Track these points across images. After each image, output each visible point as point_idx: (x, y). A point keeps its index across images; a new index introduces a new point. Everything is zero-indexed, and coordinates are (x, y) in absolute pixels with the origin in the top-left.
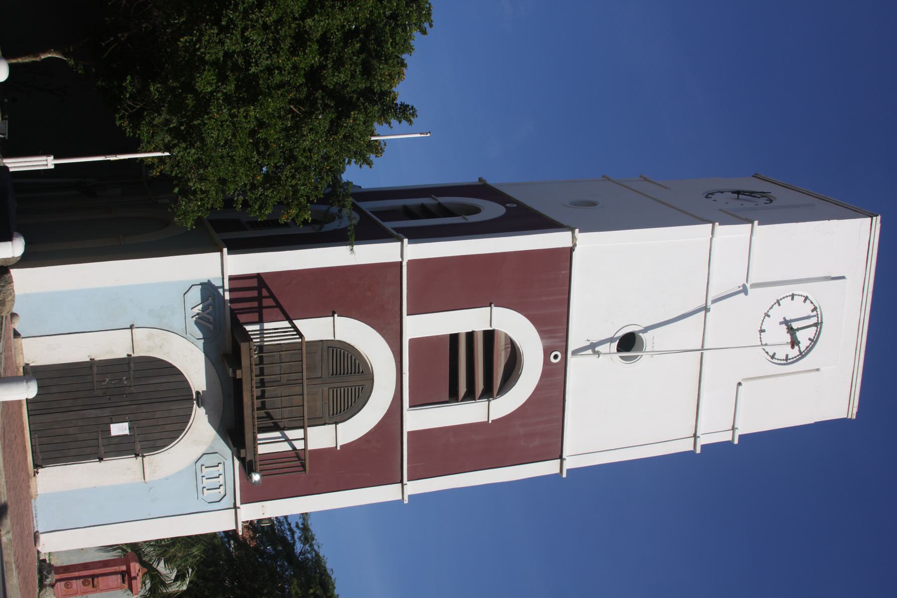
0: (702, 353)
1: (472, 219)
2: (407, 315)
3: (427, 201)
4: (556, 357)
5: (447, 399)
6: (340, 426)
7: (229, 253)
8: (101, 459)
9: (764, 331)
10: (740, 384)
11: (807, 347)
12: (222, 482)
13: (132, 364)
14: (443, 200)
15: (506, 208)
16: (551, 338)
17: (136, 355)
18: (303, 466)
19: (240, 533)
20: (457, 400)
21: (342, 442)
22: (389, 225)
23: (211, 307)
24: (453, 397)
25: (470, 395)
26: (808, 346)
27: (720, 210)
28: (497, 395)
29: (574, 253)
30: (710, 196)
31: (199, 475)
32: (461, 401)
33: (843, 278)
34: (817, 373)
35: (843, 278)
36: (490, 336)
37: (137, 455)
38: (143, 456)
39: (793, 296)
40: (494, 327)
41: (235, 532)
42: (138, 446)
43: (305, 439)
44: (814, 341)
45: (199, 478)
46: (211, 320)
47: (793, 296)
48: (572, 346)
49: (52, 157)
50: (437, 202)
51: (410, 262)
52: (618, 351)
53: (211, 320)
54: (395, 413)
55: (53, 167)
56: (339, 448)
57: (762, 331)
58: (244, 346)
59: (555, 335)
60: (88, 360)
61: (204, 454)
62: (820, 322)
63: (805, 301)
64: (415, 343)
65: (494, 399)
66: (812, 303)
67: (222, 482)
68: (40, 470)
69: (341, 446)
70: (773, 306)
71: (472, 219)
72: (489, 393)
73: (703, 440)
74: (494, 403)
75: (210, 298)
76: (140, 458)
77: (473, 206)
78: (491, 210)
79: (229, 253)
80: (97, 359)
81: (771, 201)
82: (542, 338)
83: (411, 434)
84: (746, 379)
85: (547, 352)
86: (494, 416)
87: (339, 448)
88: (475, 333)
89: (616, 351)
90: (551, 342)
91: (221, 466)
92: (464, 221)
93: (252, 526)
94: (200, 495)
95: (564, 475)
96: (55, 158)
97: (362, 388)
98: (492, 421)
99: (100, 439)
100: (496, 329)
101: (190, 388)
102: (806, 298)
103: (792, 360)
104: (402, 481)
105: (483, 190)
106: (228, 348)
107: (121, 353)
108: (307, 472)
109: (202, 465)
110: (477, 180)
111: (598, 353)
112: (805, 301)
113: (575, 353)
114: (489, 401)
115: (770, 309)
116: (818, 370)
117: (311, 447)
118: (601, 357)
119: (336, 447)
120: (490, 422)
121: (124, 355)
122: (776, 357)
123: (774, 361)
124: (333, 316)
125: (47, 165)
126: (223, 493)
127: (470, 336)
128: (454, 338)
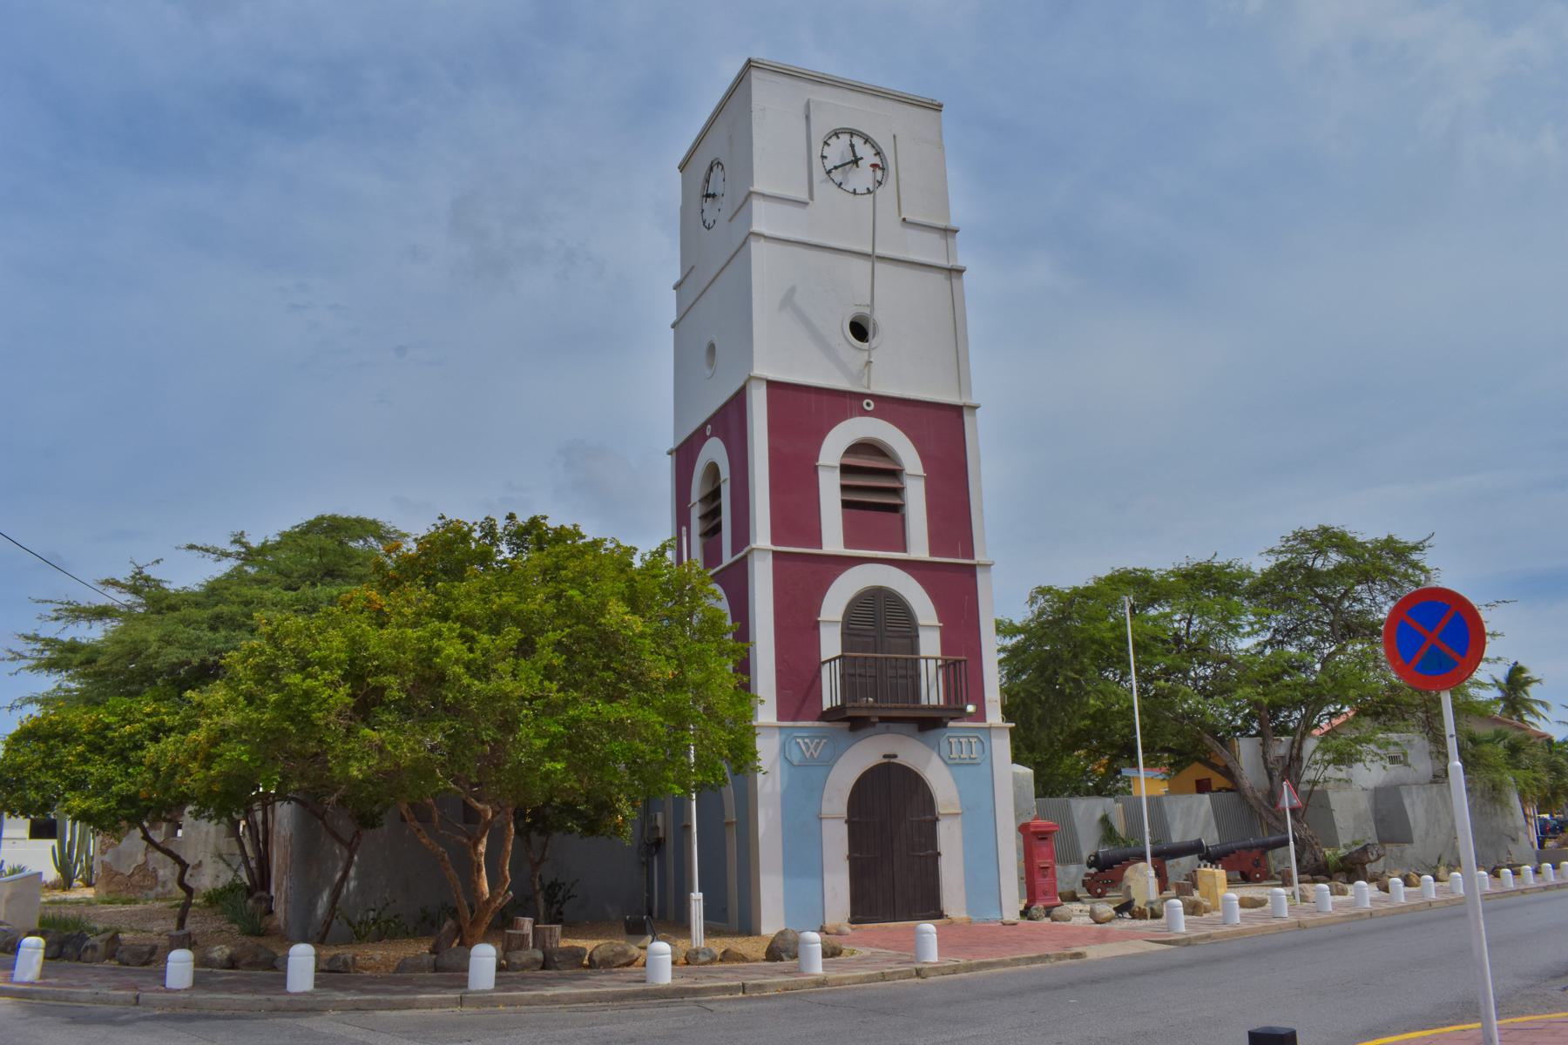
0: (879, 258)
1: (725, 473)
3: (696, 513)
4: (868, 404)
5: (897, 516)
6: (921, 621)
8: (939, 854)
9: (855, 190)
10: (904, 220)
12: (966, 740)
13: (855, 819)
14: (696, 493)
15: (711, 436)
17: (846, 816)
18: (960, 662)
19: (1013, 725)
20: (903, 506)
22: (727, 559)
23: (806, 740)
24: (897, 509)
25: (898, 492)
27: (730, 220)
29: (770, 378)
30: (707, 224)
31: (957, 761)
34: (897, 139)
36: (846, 470)
37: (937, 819)
38: (939, 813)
39: (823, 157)
40: (839, 466)
41: (1011, 730)
42: (929, 817)
43: (936, 659)
44: (867, 140)
45: (961, 762)
46: (817, 740)
47: (823, 157)
49: (693, 894)
50: (698, 503)
51: (775, 541)
52: (867, 341)
53: (817, 740)
54: (911, 567)
55: (701, 894)
56: (941, 625)
57: (854, 192)
58: (850, 713)
60: (848, 862)
61: (939, 755)
63: (829, 145)
64: (848, 543)
66: (830, 138)
67: (966, 740)
68: (945, 913)
69: (940, 622)
71: (725, 473)
72: (895, 473)
75: (798, 740)
76: (940, 818)
77: (705, 471)
78: (714, 451)
80: (847, 853)
81: (719, 163)
83: (932, 552)
84: (900, 215)
86: (919, 470)
87: (941, 625)
89: (867, 344)
91: (951, 740)
92: (728, 482)
93: (1008, 714)
94: (978, 761)
96: (692, 890)
98: (925, 472)
99: (921, 854)
101: (881, 764)
102: (826, 143)
104: (973, 567)
105: (685, 454)
106: (847, 725)
107: (843, 830)
108: (964, 657)
109: (949, 758)
110: (670, 456)
112: (829, 145)
115: (834, 181)
116: (894, 137)
117: (938, 654)
118: (872, 360)
121: (845, 828)
122: (880, 180)
124: (819, 622)
125: (699, 900)
126: (976, 740)
127: (844, 488)
128: (846, 504)
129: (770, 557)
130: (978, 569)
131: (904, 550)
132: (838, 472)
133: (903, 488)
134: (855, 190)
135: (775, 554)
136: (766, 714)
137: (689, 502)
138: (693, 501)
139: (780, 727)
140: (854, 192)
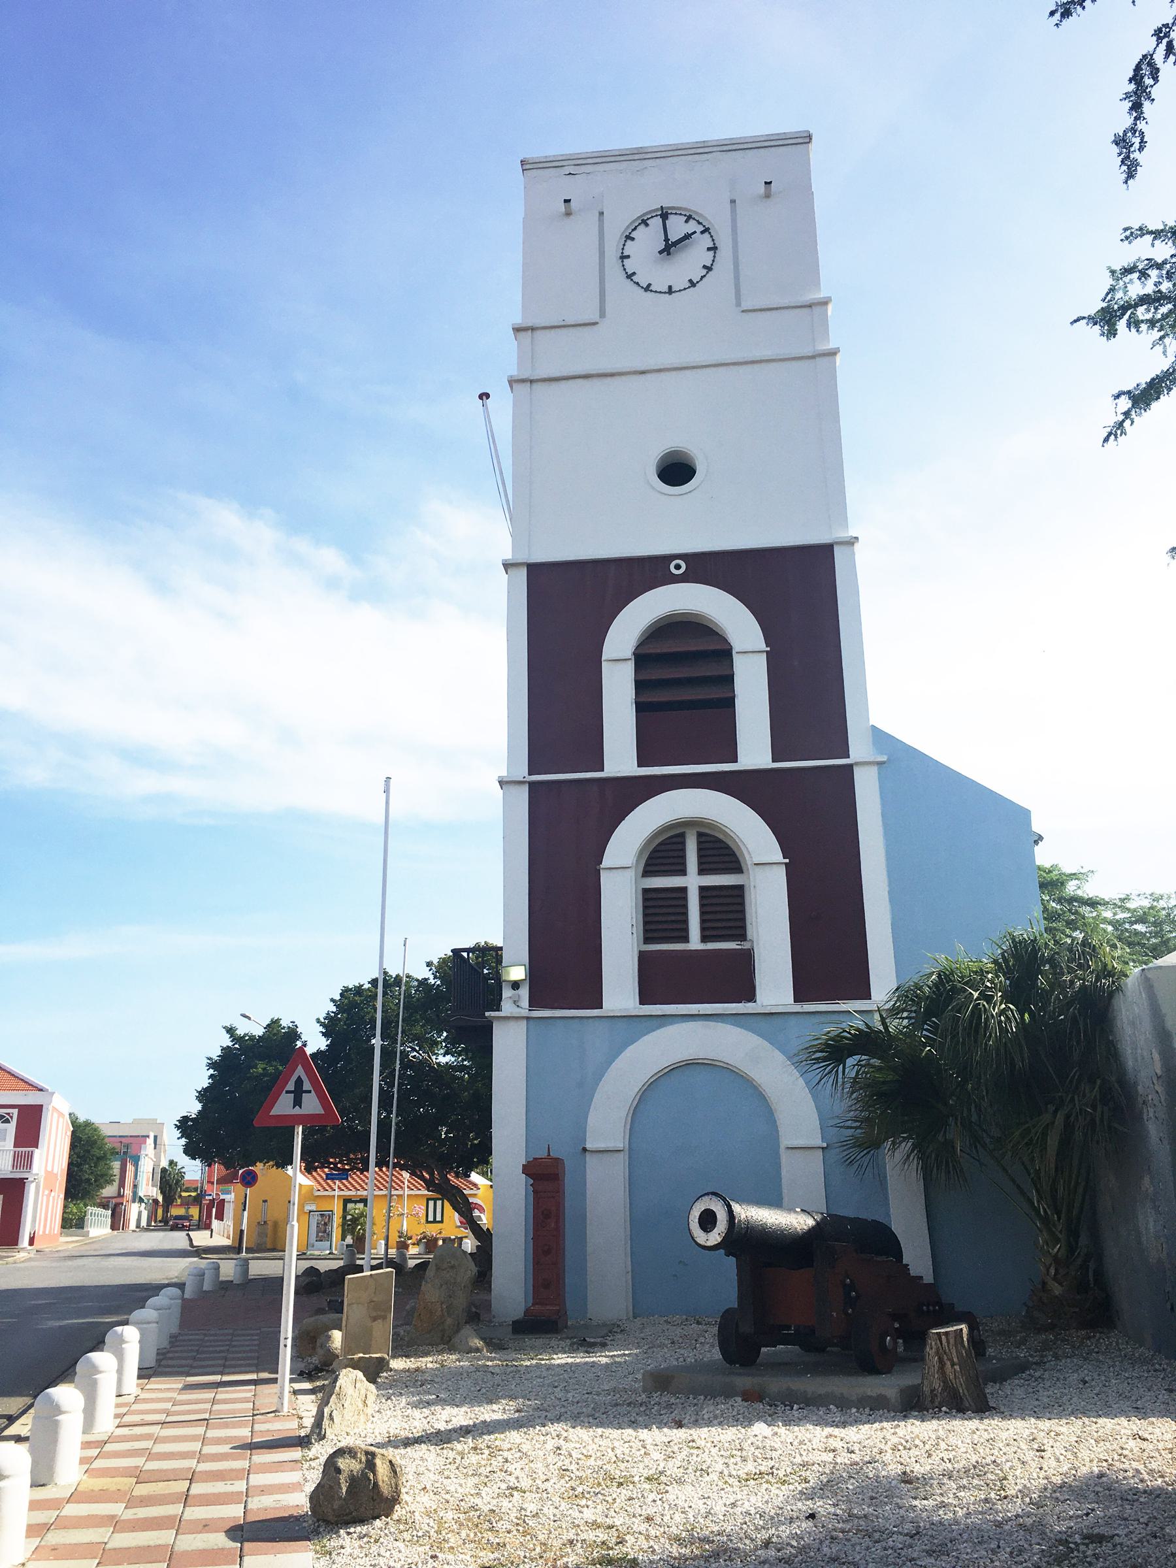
4: (678, 567)
7: (499, 1009)
21: (777, 856)
24: (729, 703)
25: (729, 680)
36: (642, 659)
56: (787, 861)
72: (724, 654)
74: (737, 644)
79: (499, 1009)
87: (787, 861)
104: (849, 768)
119: (786, 864)
120: (768, 649)
127: (640, 685)
128: (641, 708)
129: (526, 788)
130: (858, 773)
131: (735, 760)
132: (630, 668)
135: (533, 786)
136: (516, 1003)
139: (528, 1018)
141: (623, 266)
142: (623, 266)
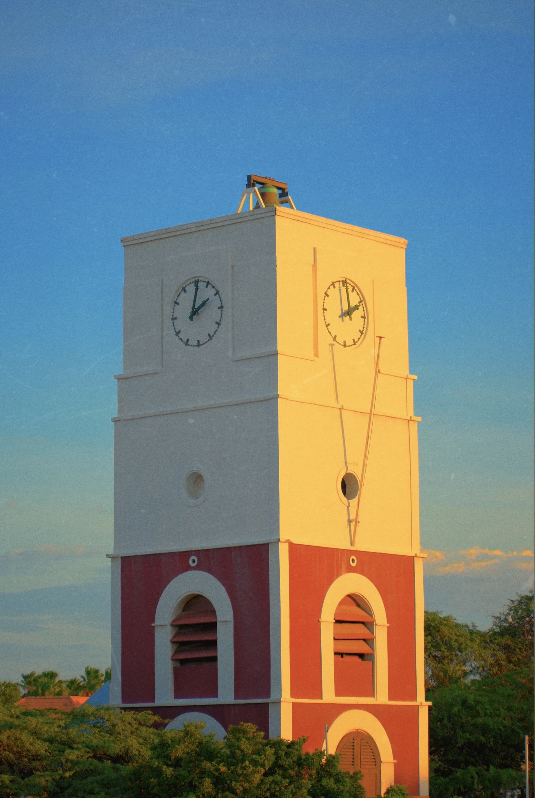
2: (322, 699)
4: (353, 560)
6: (382, 759)
9: (345, 342)
11: (358, 294)
16: (341, 567)
25: (369, 641)
26: (357, 292)
28: (372, 617)
32: (373, 650)
33: (315, 249)
35: (315, 249)
39: (325, 309)
47: (325, 309)
48: (347, 546)
59: (340, 560)
62: (362, 299)
65: (375, 621)
70: (329, 332)
72: (369, 624)
73: (411, 413)
82: (341, 575)
83: (390, 699)
85: (350, 570)
88: (336, 638)
90: (344, 567)
95: (425, 555)
97: (363, 739)
98: (388, 622)
100: (333, 617)
102: (326, 294)
103: (365, 313)
111: (357, 522)
113: (352, 544)
114: (376, 624)
115: (331, 335)
120: (389, 625)
123: (364, 332)
133: (373, 639)
134: (345, 342)
137: (154, 622)
138: (157, 622)
140: (345, 345)
141: (349, 346)
142: (349, 346)
